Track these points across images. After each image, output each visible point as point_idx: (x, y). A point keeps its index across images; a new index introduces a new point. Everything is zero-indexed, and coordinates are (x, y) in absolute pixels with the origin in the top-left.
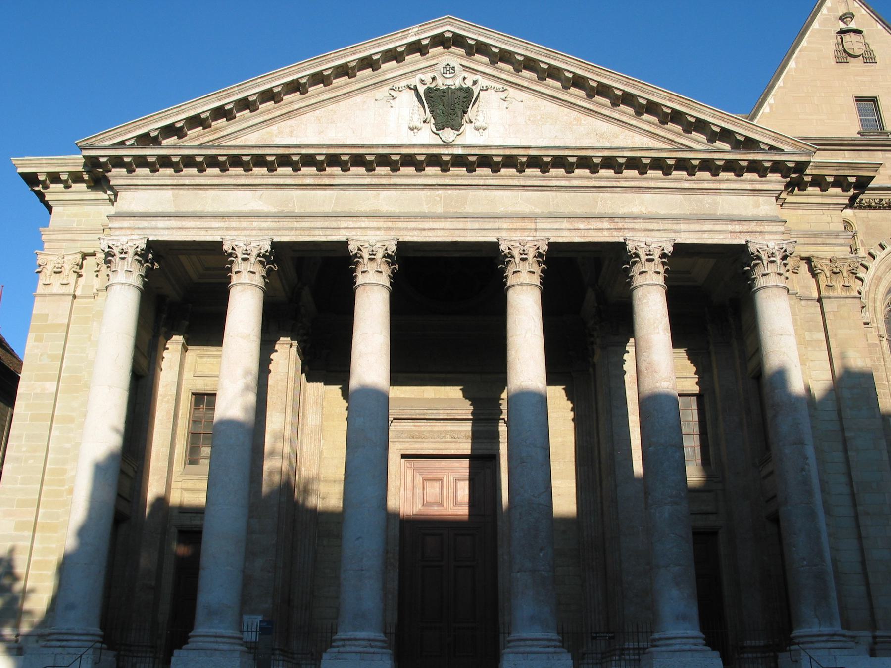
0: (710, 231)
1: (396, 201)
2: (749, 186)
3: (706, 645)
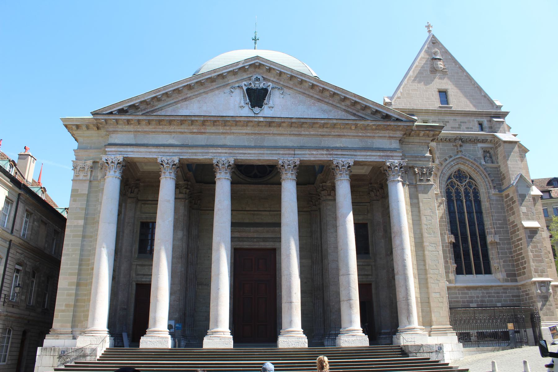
0: (370, 155)
2: (387, 135)
3: (363, 333)
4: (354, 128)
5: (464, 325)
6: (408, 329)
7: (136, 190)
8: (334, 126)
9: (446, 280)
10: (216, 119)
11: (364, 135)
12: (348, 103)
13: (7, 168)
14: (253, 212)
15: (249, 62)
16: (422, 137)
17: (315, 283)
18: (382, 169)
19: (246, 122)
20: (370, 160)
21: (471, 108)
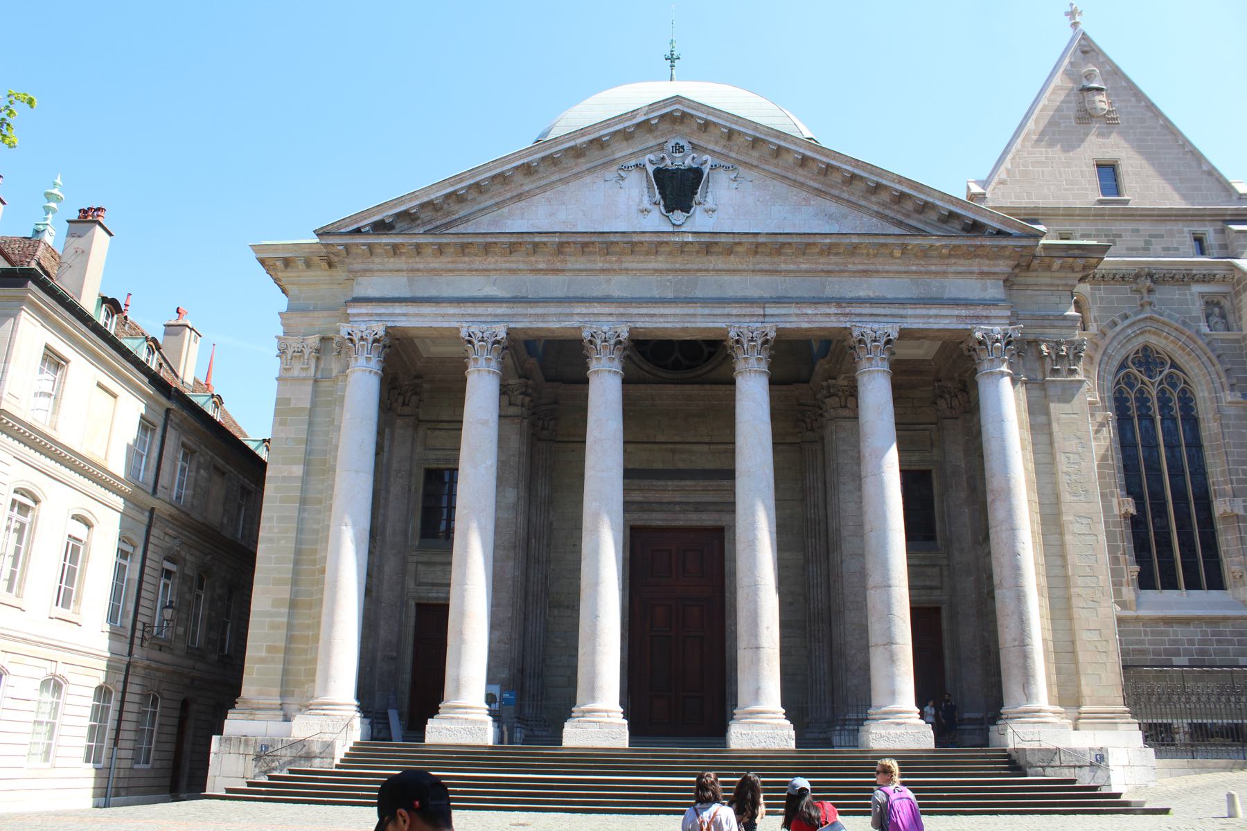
0: (936, 316)
1: (628, 286)
2: (976, 269)
4: (899, 255)
5: (1158, 706)
6: (1026, 712)
7: (414, 398)
8: (853, 250)
9: (1116, 602)
10: (587, 239)
11: (922, 269)
12: (885, 196)
13: (143, 355)
14: (672, 446)
15: (658, 110)
16: (1058, 271)
17: (812, 606)
18: (963, 346)
19: (654, 246)
20: (936, 326)
21: (1175, 202)
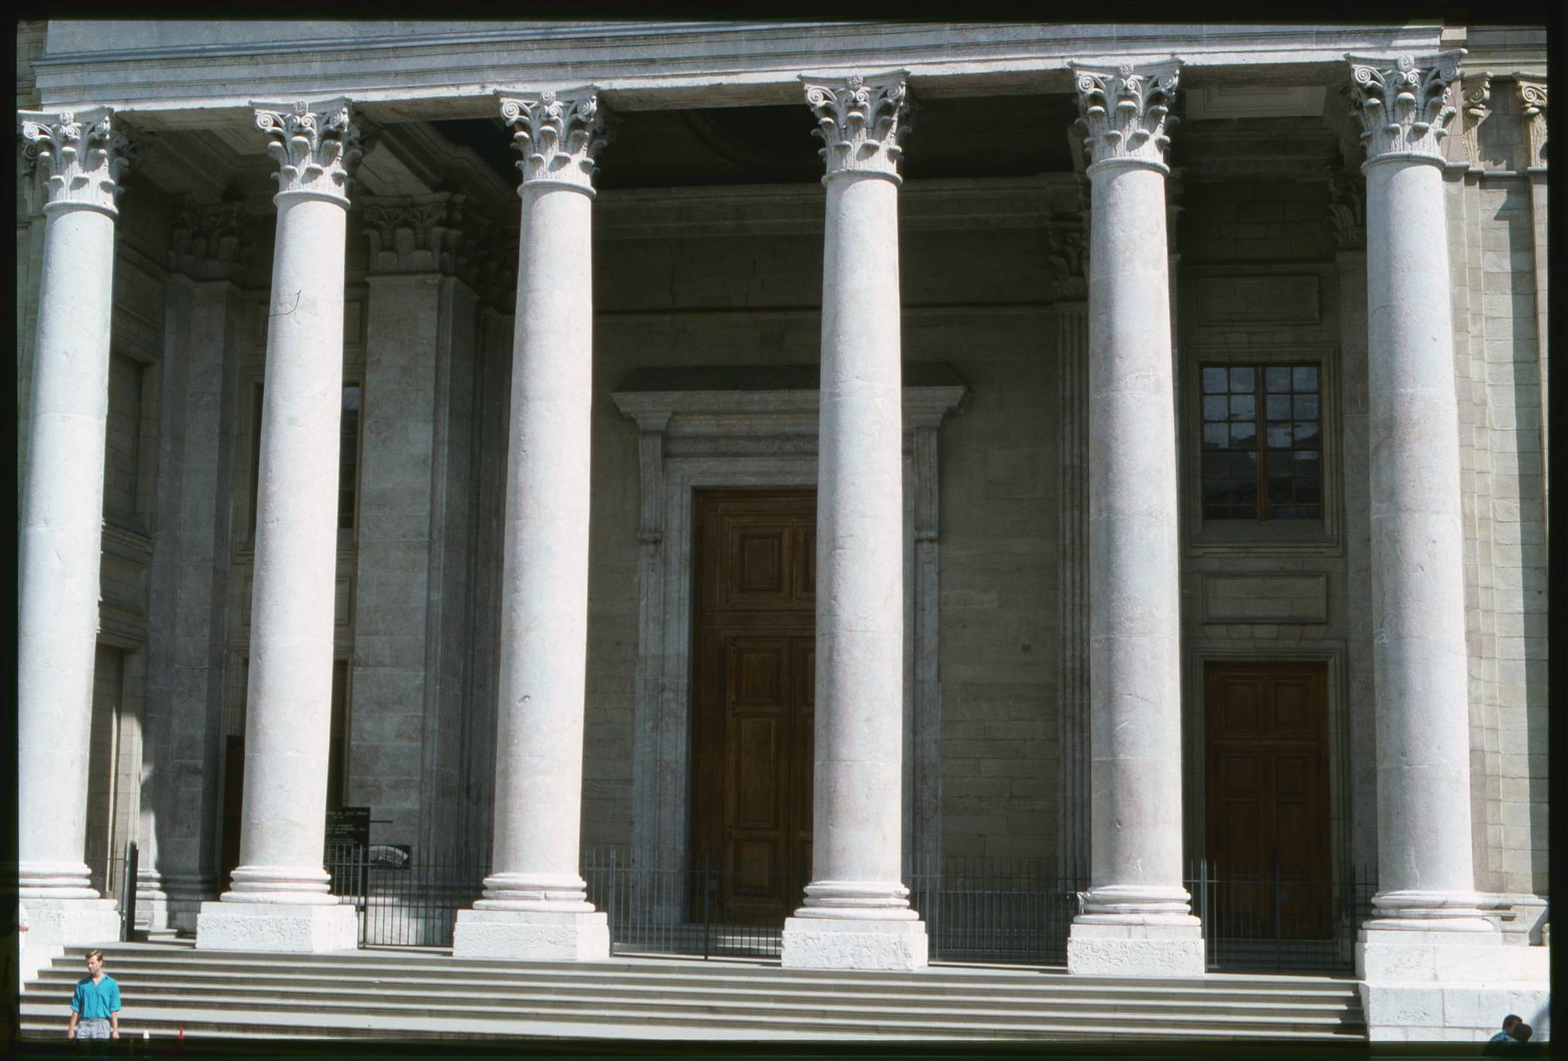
17: (1069, 654)
